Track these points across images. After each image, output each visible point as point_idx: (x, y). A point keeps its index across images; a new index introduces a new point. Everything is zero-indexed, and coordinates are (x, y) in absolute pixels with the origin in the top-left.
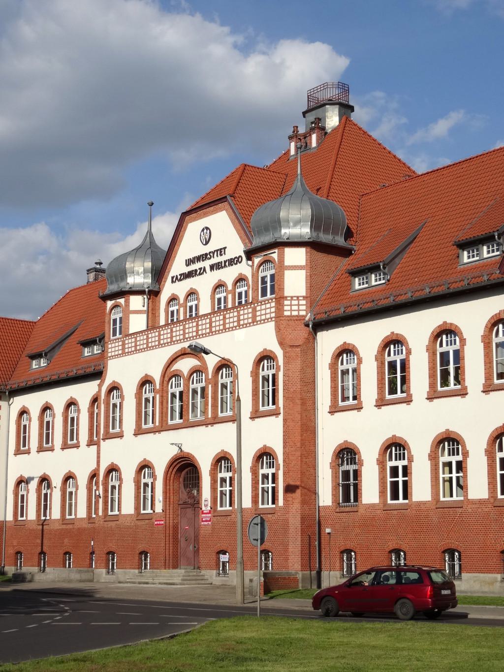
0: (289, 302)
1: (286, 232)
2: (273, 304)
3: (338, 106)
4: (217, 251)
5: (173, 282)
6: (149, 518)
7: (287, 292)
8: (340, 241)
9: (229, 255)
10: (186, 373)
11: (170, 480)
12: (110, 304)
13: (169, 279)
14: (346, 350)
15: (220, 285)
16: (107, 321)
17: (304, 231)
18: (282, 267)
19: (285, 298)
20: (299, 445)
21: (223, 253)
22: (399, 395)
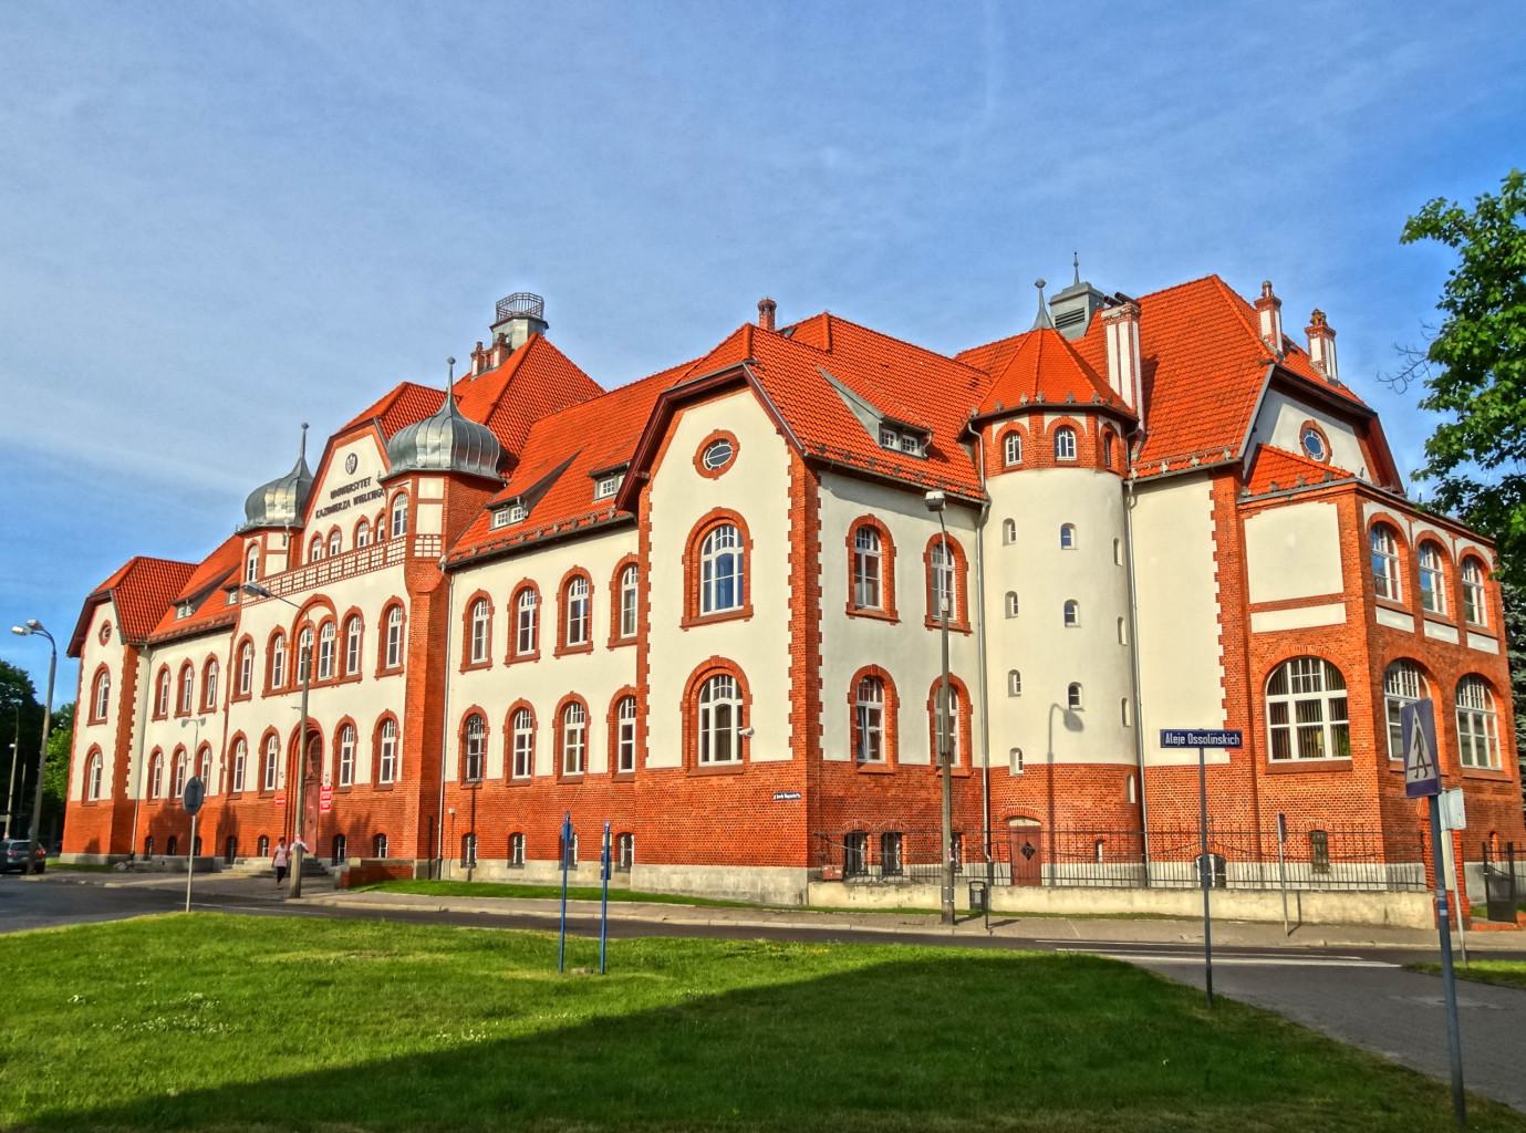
1: (422, 460)
2: (404, 544)
3: (526, 321)
5: (317, 517)
6: (271, 795)
7: (419, 531)
8: (489, 471)
10: (317, 624)
12: (247, 541)
13: (314, 514)
14: (480, 598)
15: (363, 521)
16: (243, 563)
17: (444, 459)
18: (415, 501)
19: (418, 537)
20: (422, 709)
22: (530, 651)
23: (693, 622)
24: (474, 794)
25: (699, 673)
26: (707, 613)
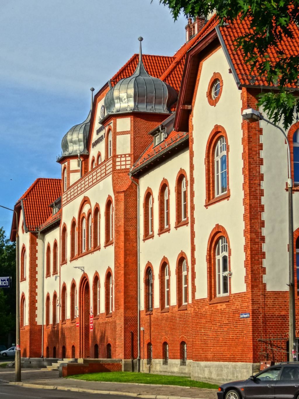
0: (120, 159)
1: (118, 106)
11: (82, 293)
17: (131, 105)
23: (210, 202)
24: (150, 317)
25: (212, 235)
26: (218, 196)
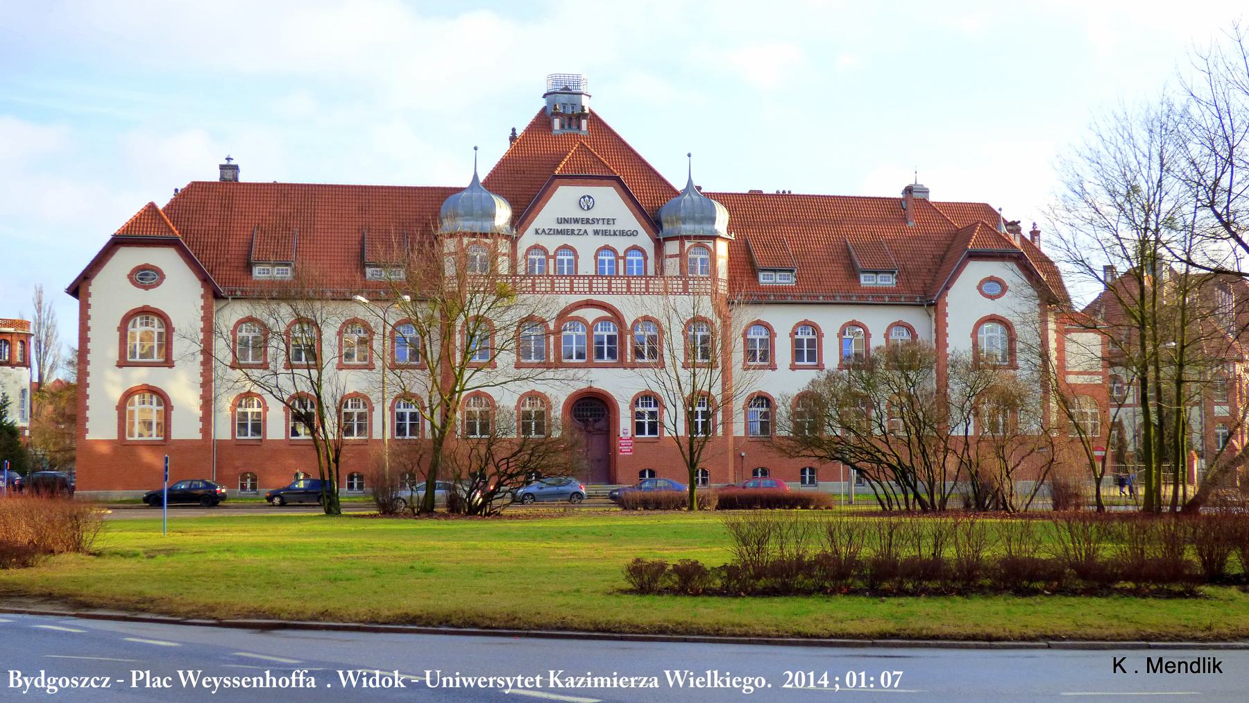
4: (603, 219)
5: (537, 232)
9: (617, 227)
21: (611, 222)
